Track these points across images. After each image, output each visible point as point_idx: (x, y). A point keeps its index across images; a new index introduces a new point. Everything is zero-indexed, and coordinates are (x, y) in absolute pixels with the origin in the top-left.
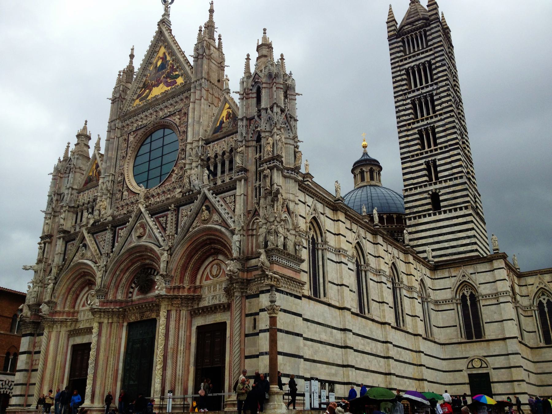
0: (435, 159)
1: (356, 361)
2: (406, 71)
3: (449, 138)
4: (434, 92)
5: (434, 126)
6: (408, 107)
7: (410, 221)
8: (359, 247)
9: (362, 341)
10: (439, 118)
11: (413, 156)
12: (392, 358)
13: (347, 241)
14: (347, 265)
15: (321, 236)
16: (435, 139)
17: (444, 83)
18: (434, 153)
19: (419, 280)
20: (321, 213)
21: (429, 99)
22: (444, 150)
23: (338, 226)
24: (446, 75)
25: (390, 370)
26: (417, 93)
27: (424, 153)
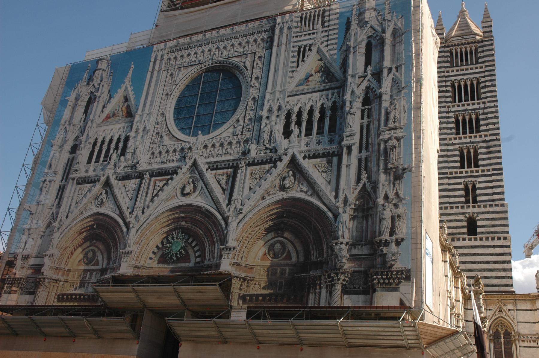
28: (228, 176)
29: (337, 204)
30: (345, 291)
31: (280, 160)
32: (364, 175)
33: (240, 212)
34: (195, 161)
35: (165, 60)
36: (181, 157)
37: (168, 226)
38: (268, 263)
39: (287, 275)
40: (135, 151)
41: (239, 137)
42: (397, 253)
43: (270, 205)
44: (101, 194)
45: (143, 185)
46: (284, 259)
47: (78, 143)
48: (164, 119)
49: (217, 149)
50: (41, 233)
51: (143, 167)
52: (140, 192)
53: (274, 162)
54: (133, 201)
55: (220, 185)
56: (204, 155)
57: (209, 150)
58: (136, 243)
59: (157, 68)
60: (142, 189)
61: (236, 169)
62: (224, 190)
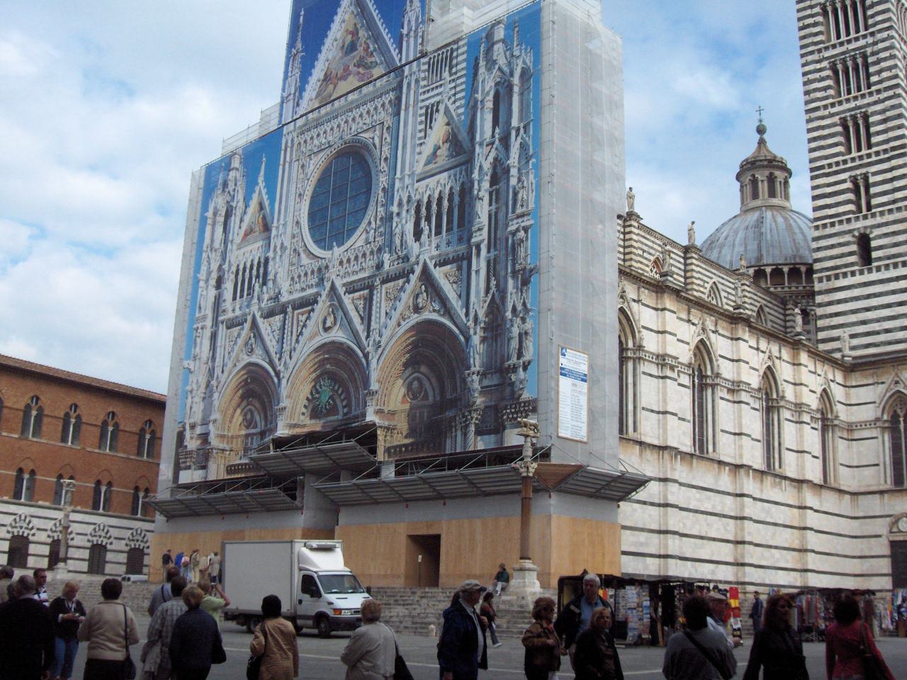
0: (867, 172)
1: (684, 524)
2: (822, 9)
3: (891, 134)
4: (869, 50)
5: (867, 111)
6: (824, 74)
7: (821, 284)
8: (702, 349)
9: (698, 496)
10: (875, 98)
11: (830, 166)
12: (751, 519)
13: (678, 340)
14: (676, 380)
15: (634, 337)
16: (869, 135)
17: (885, 35)
18: (866, 161)
19: (819, 390)
20: (634, 301)
21: (860, 61)
22: (882, 157)
23: (664, 318)
24: (889, 19)
25: (743, 537)
26: (839, 50)
27: (849, 161)
28: (365, 299)
29: (468, 324)
30: (479, 432)
31: (413, 272)
32: (493, 282)
33: (378, 345)
34: (333, 283)
35: (295, 146)
36: (319, 279)
37: (314, 371)
38: (407, 406)
39: (425, 419)
40: (275, 277)
41: (372, 243)
42: (524, 380)
43: (407, 331)
44: (250, 338)
45: (287, 322)
46: (423, 399)
47: (221, 274)
48: (299, 230)
49: (352, 264)
50: (203, 395)
51: (285, 298)
52: (286, 331)
53: (405, 274)
54: (280, 343)
55: (358, 312)
56: (341, 274)
57: (344, 267)
58: (289, 396)
59: (288, 159)
60: (286, 327)
61: (371, 288)
62: (362, 319)
